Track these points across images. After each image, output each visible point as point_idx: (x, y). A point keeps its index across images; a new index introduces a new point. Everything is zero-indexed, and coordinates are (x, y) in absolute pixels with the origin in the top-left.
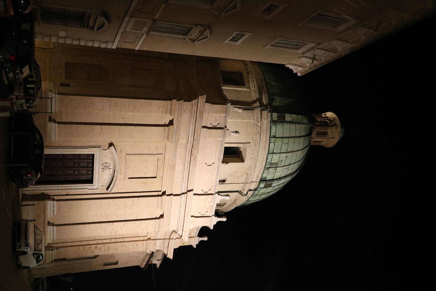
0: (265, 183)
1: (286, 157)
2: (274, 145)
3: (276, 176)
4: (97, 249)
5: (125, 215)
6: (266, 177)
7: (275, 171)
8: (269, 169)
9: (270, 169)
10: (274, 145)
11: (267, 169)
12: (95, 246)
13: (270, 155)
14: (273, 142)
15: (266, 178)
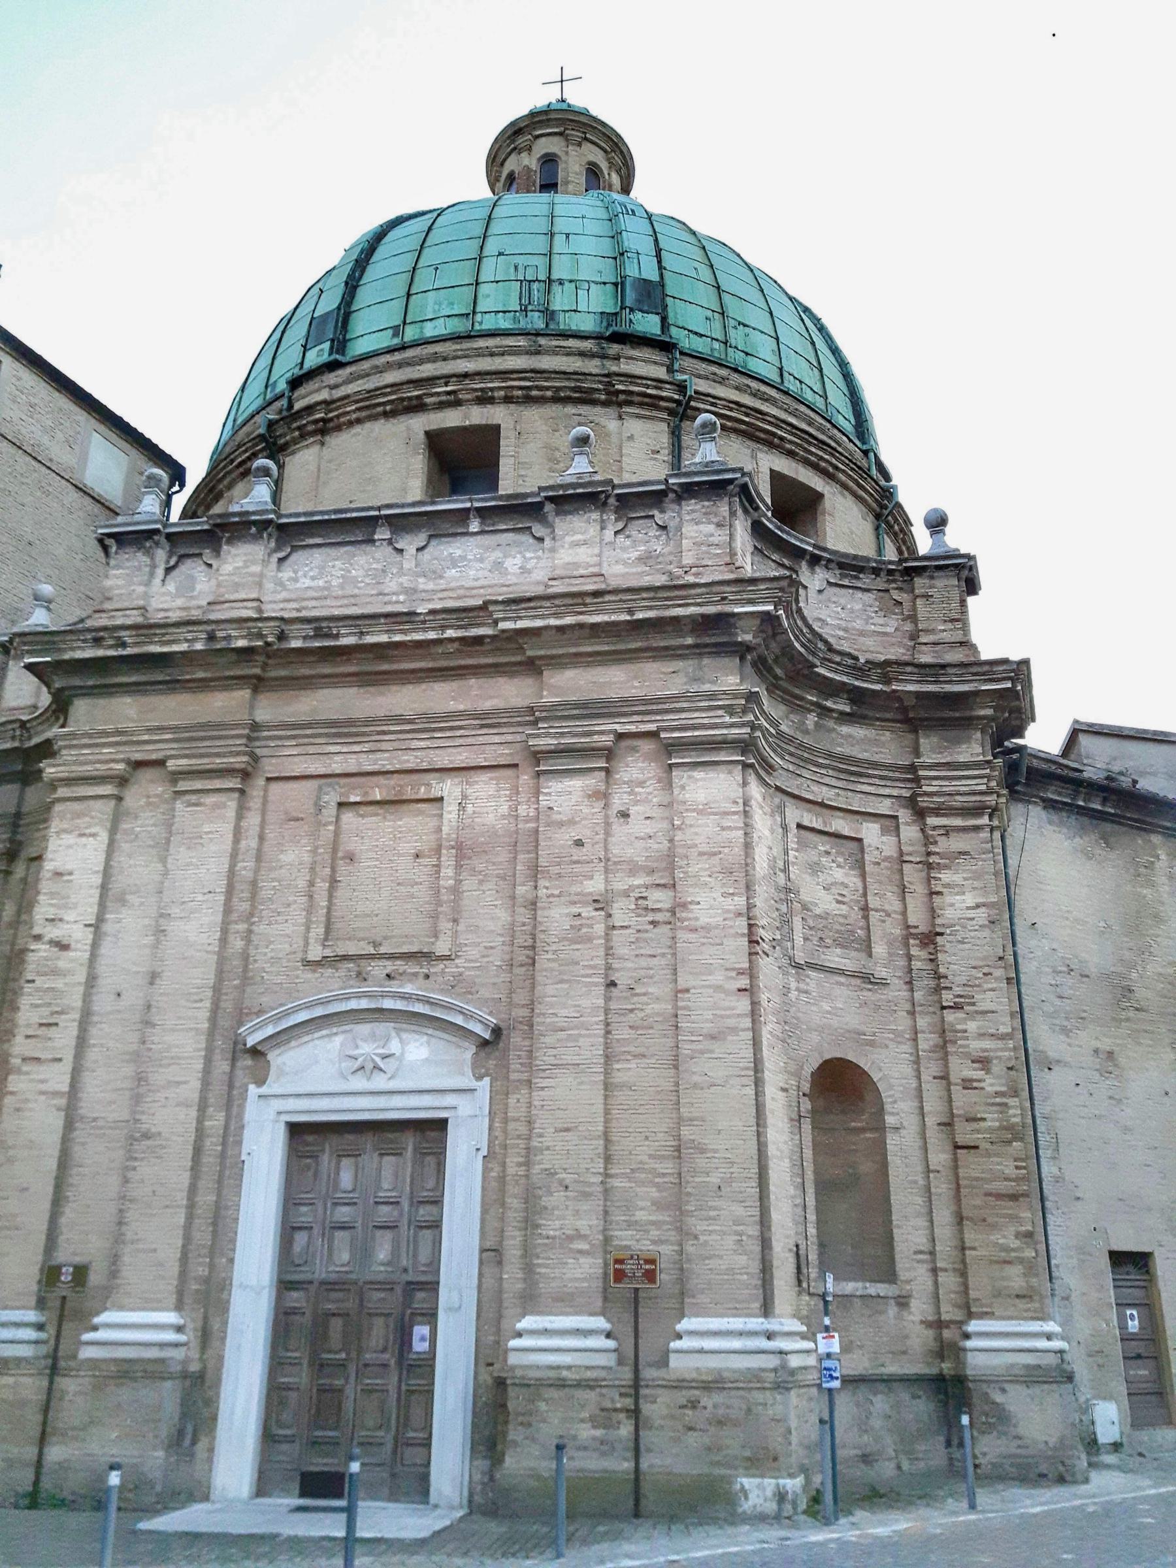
0: (632, 310)
1: (500, 254)
2: (431, 320)
3: (600, 272)
4: (979, 1081)
5: (639, 931)
6: (598, 317)
7: (571, 281)
8: (553, 312)
9: (556, 306)
10: (431, 320)
11: (552, 319)
12: (957, 1091)
13: (481, 323)
14: (422, 328)
15: (602, 313)
